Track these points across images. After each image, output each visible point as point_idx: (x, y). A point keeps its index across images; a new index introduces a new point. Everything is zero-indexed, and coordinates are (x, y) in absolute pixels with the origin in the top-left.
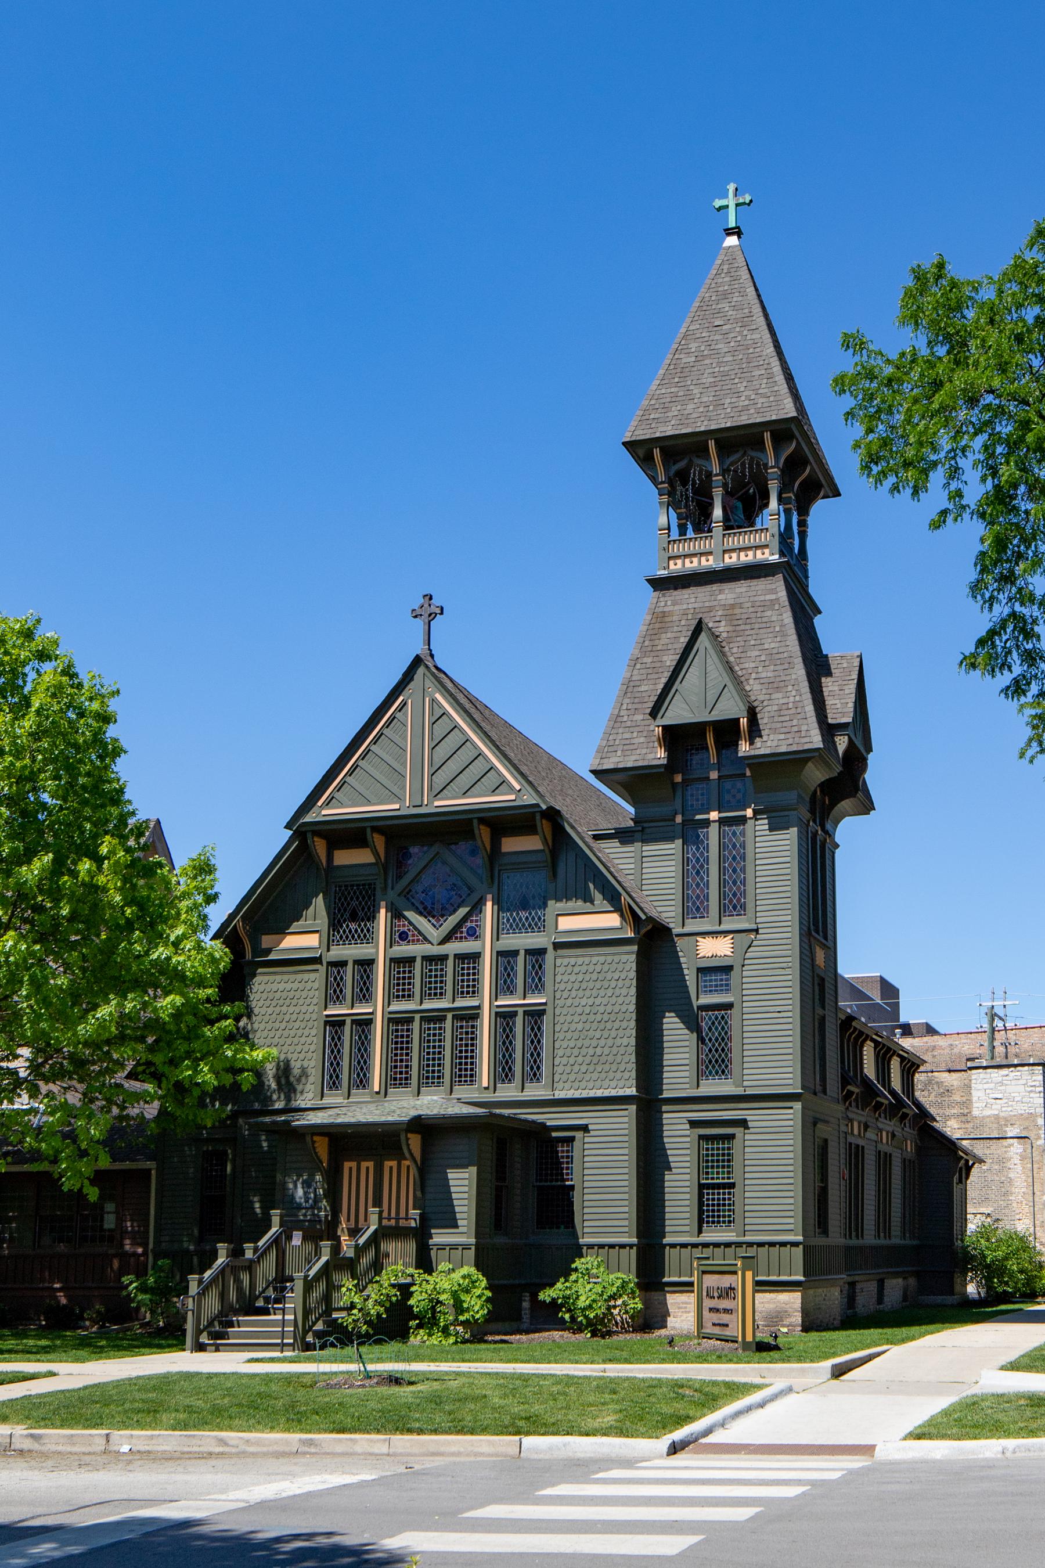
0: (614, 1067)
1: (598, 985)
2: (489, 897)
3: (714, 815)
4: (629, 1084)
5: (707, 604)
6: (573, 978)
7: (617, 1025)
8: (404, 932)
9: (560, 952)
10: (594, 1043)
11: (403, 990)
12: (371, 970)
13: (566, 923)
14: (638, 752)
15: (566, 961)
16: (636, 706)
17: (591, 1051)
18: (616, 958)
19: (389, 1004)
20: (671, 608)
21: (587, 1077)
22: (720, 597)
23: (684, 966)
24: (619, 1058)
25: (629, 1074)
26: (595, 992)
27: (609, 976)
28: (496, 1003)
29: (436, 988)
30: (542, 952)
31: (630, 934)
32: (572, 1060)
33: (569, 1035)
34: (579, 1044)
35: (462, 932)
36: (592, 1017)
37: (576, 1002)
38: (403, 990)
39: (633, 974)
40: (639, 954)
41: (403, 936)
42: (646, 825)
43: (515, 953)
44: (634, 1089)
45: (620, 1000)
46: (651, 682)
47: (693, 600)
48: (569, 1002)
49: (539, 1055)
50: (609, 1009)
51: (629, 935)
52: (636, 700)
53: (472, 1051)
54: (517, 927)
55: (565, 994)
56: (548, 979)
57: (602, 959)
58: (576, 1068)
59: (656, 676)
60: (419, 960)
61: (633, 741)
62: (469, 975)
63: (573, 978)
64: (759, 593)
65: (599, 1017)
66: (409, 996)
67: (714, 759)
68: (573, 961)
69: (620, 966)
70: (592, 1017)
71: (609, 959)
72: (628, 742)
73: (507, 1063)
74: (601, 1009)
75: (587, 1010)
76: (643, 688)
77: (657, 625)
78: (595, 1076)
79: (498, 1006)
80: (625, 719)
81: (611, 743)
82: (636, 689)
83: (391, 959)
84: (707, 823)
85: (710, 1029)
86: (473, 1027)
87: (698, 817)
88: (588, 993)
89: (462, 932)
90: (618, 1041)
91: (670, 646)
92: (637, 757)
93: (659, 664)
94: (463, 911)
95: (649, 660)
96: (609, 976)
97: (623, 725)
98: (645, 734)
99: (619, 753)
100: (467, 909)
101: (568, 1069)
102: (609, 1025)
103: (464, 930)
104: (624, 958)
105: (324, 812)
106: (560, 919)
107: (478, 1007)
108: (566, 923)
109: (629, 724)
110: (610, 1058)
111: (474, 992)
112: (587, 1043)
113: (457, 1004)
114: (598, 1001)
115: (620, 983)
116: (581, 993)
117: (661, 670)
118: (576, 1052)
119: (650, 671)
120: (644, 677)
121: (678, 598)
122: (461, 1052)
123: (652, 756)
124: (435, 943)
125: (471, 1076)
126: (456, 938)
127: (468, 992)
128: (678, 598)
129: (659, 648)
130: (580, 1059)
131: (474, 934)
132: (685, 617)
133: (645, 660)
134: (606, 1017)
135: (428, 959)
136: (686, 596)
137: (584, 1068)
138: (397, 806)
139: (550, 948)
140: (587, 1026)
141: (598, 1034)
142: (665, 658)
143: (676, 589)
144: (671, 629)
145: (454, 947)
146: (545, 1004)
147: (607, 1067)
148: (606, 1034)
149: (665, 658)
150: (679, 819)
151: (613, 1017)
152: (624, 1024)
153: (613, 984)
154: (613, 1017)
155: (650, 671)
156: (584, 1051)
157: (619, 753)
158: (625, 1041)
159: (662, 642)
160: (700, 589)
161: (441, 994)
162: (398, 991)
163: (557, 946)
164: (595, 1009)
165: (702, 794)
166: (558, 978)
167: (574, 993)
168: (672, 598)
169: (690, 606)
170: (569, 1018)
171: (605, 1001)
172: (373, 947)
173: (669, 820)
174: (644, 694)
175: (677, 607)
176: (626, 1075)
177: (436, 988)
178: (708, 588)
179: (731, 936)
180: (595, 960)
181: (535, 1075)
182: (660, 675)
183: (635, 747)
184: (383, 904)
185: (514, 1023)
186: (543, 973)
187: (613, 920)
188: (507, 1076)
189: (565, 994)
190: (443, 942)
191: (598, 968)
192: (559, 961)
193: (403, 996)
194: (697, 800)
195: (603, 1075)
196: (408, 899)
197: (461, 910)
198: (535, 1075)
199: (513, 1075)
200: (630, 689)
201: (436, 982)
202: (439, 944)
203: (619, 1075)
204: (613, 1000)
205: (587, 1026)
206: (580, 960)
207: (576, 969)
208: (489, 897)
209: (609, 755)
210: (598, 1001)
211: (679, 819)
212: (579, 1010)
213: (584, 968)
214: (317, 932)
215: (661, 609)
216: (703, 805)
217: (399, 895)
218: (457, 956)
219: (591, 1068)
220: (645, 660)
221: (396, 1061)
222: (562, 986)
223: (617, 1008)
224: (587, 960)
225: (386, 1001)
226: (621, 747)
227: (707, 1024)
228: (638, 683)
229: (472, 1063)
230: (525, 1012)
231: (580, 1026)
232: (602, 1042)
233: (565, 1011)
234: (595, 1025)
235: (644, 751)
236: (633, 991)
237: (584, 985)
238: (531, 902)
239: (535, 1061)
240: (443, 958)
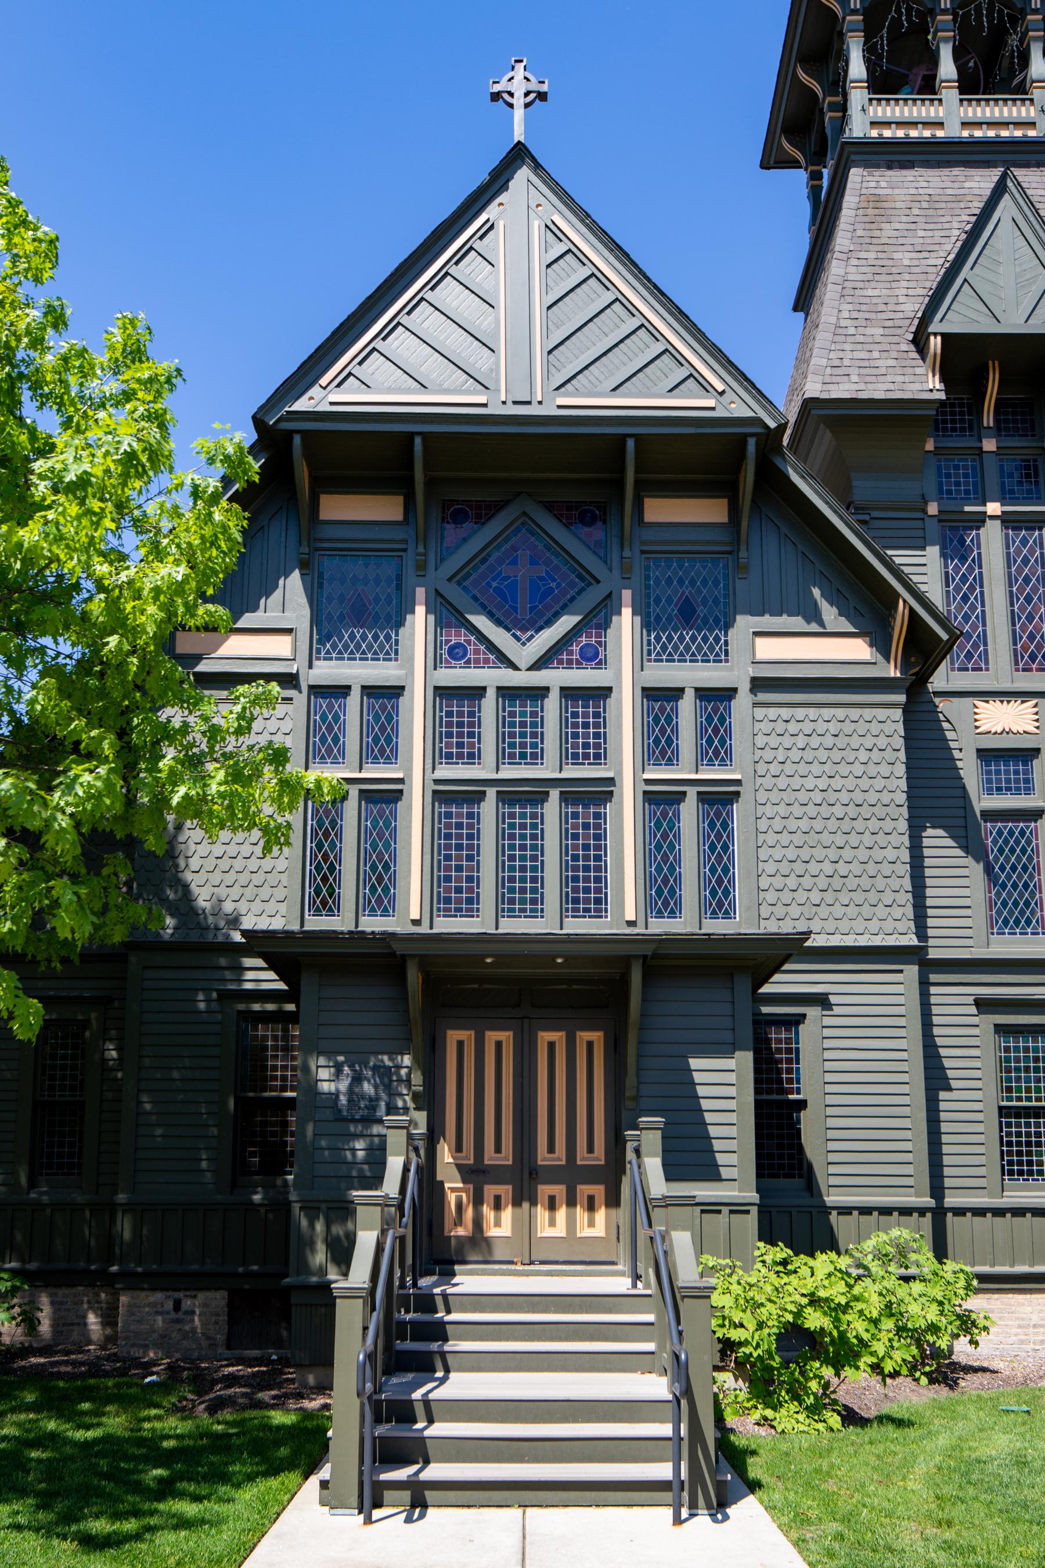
0: (873, 897)
1: (836, 756)
2: (627, 595)
3: (993, 508)
4: (902, 927)
5: (949, 192)
6: (787, 742)
7: (874, 825)
8: (458, 645)
9: (762, 697)
10: (833, 854)
11: (460, 745)
12: (396, 708)
13: (768, 649)
14: (889, 378)
15: (773, 713)
16: (867, 315)
17: (829, 870)
18: (868, 713)
19: (434, 769)
20: (889, 191)
21: (823, 911)
22: (967, 185)
23: (952, 745)
24: (880, 883)
25: (901, 910)
26: (828, 768)
27: (855, 741)
28: (646, 776)
29: (523, 745)
30: (730, 693)
31: (893, 672)
32: (792, 882)
33: (785, 839)
34: (805, 854)
35: (571, 653)
36: (825, 811)
37: (796, 784)
38: (460, 745)
39: (899, 743)
40: (908, 710)
41: (457, 653)
42: (874, 514)
43: (677, 693)
44: (914, 937)
45: (879, 784)
46: (880, 285)
47: (925, 184)
48: (782, 783)
49: (726, 870)
50: (858, 797)
51: (892, 675)
52: (864, 308)
53: (598, 858)
54: (667, 654)
55: (774, 769)
56: (739, 742)
57: (840, 713)
58: (801, 896)
59: (890, 278)
60: (491, 693)
61: (873, 363)
62: (586, 725)
63: (787, 742)
64: (1034, 185)
65: (839, 811)
66: (471, 756)
67: (988, 419)
68: (786, 713)
69: (875, 728)
70: (825, 811)
71: (854, 713)
72: (866, 364)
73: (665, 881)
74: (844, 797)
75: (818, 797)
76: (870, 292)
77: (870, 211)
78: (838, 911)
79: (648, 782)
80: (852, 331)
81: (837, 363)
82: (858, 292)
83: (436, 688)
84: (980, 520)
85: (1001, 851)
86: (597, 816)
87: (967, 509)
88: (816, 769)
89: (571, 653)
90: (878, 854)
91: (901, 241)
92: (891, 387)
93: (890, 263)
94: (566, 622)
95: (873, 255)
96: (855, 741)
97: (850, 339)
98: (894, 355)
99: (854, 378)
100: (577, 619)
101: (786, 897)
102: (859, 825)
103: (575, 648)
104: (881, 713)
105: (334, 397)
106: (760, 641)
107: (611, 781)
108: (768, 649)
109: (861, 339)
110: (865, 882)
111: (597, 756)
112: (819, 853)
113: (564, 775)
114: (837, 783)
115: (876, 755)
116: (803, 769)
117: (894, 270)
118: (799, 867)
119: (877, 270)
120: (870, 277)
121: (894, 179)
122: (575, 858)
123: (917, 386)
124: (523, 664)
125: (598, 901)
126: (561, 662)
127: (586, 756)
128: (894, 179)
129: (883, 241)
130: (807, 881)
131: (593, 657)
132: (917, 205)
133: (862, 255)
134: (852, 811)
135: (505, 693)
136: (912, 179)
137: (815, 897)
138: (482, 399)
139: (744, 688)
140: (818, 825)
141: (840, 840)
142: (896, 256)
143: (890, 167)
144: (898, 219)
145: (555, 677)
146: (738, 782)
147: (859, 897)
148: (854, 839)
149: (896, 256)
150: (933, 509)
151: (866, 812)
152: (888, 825)
153: (863, 756)
154: (866, 812)
155: (877, 270)
156: (814, 868)
157: (854, 378)
158: (891, 854)
159: (884, 233)
160: (930, 172)
161: (534, 756)
162: (449, 745)
163: (758, 684)
164: (832, 797)
165: (966, 476)
166: (760, 741)
167: (789, 768)
168: (887, 179)
169: (921, 191)
170: (782, 810)
171: (850, 783)
172: (401, 667)
173: (915, 510)
174: (875, 300)
175: (896, 191)
176: (897, 913)
177: (523, 745)
178: (946, 171)
179: (1033, 702)
180: (827, 713)
181: (720, 904)
182: (898, 277)
183: (883, 371)
184: (420, 593)
185: (677, 815)
186: (729, 731)
187: (859, 649)
188: (666, 904)
189: (774, 769)
190: (535, 666)
191: (833, 728)
192: (760, 713)
193: (460, 756)
194: (958, 484)
195: (852, 911)
196: (465, 589)
197: (564, 618)
198: (720, 904)
199: (679, 904)
200: (846, 292)
201: (523, 735)
202: (529, 669)
203: (882, 912)
204: (865, 783)
205: (818, 825)
206: (800, 713)
207: (793, 728)
208: (627, 595)
209: (835, 379)
210: (837, 783)
211: (933, 509)
212: (803, 796)
213: (808, 728)
214: (288, 631)
215: (873, 191)
216: (967, 492)
217: (449, 580)
218: (569, 693)
219: (829, 897)
220: (862, 255)
221: (448, 868)
222: (768, 755)
223: (872, 797)
224: (813, 713)
225: (429, 761)
226: (854, 371)
227: (995, 842)
228: (861, 285)
229: (598, 880)
230: (699, 793)
231: (804, 824)
232: (847, 854)
233: (774, 796)
234: (832, 825)
235: (900, 379)
236: (901, 770)
237: (809, 755)
238: (701, 611)
239: (719, 881)
240: (540, 693)
